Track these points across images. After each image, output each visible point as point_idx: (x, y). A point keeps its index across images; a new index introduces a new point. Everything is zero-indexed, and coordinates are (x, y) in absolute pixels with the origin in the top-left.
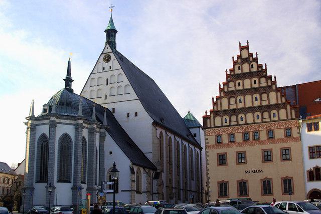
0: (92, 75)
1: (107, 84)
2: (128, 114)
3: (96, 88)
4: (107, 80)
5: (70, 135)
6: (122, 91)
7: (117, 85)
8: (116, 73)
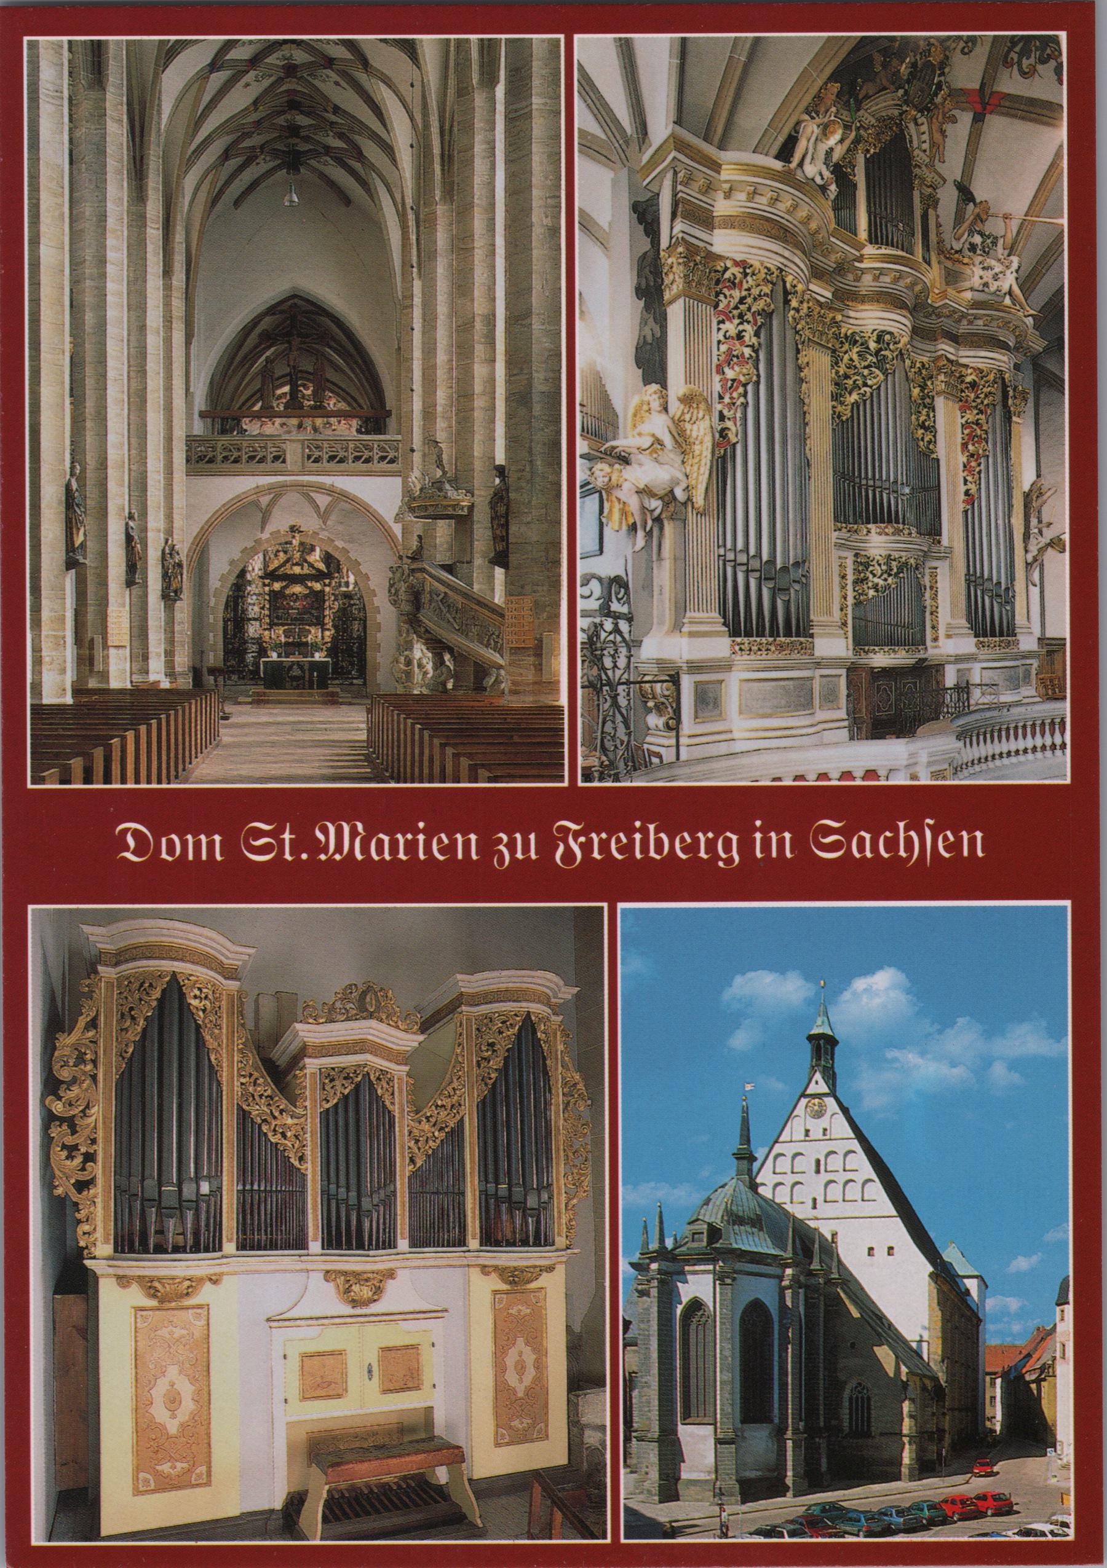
0: (777, 1145)
1: (818, 1171)
2: (871, 1249)
3: (789, 1179)
4: (818, 1162)
5: (768, 1304)
6: (854, 1191)
7: (842, 1177)
8: (841, 1147)
